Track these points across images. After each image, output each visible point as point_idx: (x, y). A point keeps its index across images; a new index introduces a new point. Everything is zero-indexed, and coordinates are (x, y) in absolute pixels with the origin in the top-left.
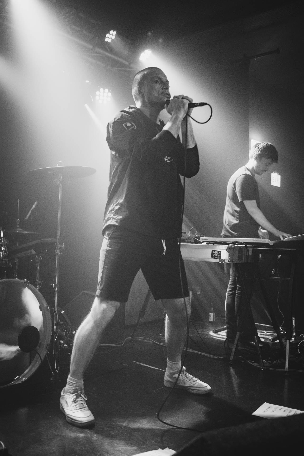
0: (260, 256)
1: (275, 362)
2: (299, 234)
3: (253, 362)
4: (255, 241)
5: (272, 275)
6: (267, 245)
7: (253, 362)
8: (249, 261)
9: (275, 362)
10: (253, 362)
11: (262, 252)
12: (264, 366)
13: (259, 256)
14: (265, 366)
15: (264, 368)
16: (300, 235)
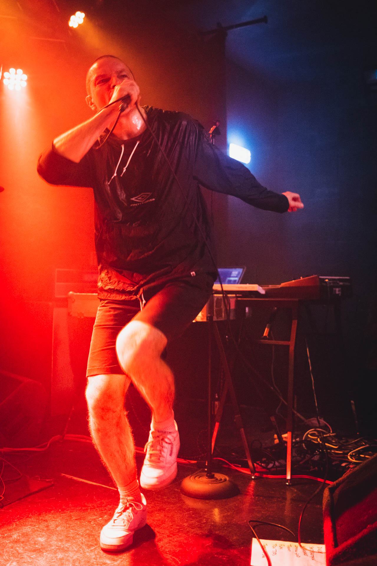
0: (247, 309)
1: (271, 465)
2: (301, 277)
3: (240, 466)
4: (239, 288)
5: (265, 338)
6: (256, 293)
7: (239, 467)
8: (232, 317)
9: (271, 465)
10: (239, 467)
11: (248, 304)
12: (256, 472)
13: (245, 310)
14: (258, 472)
15: (257, 474)
16: (304, 279)
